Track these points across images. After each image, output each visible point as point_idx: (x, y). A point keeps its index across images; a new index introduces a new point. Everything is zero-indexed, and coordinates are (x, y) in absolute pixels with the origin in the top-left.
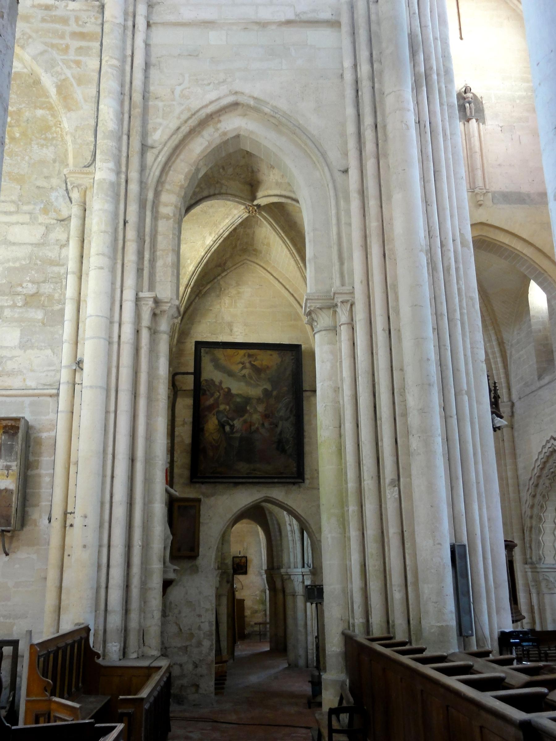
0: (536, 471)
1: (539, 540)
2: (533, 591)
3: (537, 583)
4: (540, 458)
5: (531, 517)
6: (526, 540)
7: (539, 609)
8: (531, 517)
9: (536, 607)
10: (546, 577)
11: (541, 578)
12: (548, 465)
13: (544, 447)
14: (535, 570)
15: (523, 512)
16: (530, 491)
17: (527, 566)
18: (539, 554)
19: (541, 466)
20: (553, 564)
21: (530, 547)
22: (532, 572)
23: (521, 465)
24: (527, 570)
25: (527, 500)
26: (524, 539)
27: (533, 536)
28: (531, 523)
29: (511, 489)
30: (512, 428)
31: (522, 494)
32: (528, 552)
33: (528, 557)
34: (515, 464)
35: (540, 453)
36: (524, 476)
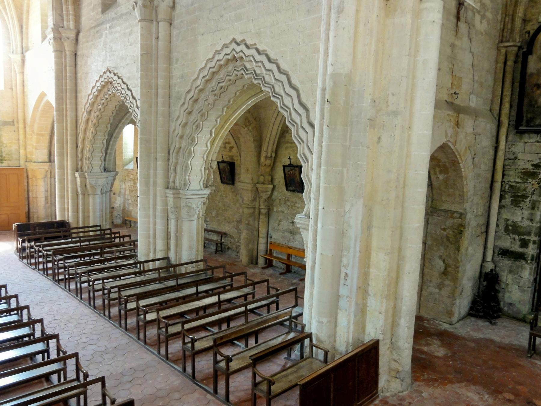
0: (199, 82)
1: (187, 163)
2: (172, 217)
3: (177, 209)
4: (209, 65)
5: (181, 137)
6: (171, 161)
7: (176, 236)
8: (181, 137)
9: (173, 235)
10: (189, 204)
11: (183, 204)
12: (217, 77)
13: (218, 52)
14: (177, 197)
15: (172, 130)
16: (186, 106)
17: (168, 191)
18: (185, 179)
19: (207, 78)
20: (198, 190)
21: (175, 170)
22: (174, 198)
23: (176, 73)
24: (168, 195)
25: (179, 117)
26: (169, 160)
27: (180, 158)
28: (180, 143)
29: (160, 100)
30: (171, 24)
31: (173, 109)
32: (172, 175)
33: (171, 180)
34: (169, 71)
35: (209, 60)
36: (180, 88)
